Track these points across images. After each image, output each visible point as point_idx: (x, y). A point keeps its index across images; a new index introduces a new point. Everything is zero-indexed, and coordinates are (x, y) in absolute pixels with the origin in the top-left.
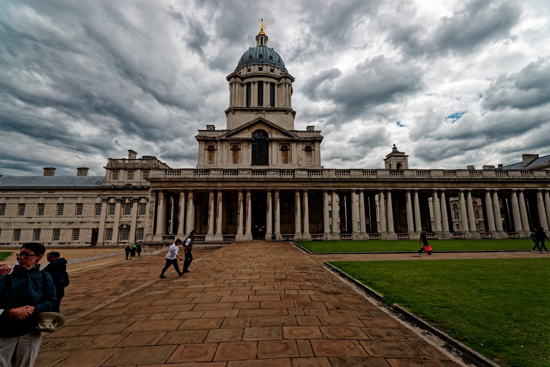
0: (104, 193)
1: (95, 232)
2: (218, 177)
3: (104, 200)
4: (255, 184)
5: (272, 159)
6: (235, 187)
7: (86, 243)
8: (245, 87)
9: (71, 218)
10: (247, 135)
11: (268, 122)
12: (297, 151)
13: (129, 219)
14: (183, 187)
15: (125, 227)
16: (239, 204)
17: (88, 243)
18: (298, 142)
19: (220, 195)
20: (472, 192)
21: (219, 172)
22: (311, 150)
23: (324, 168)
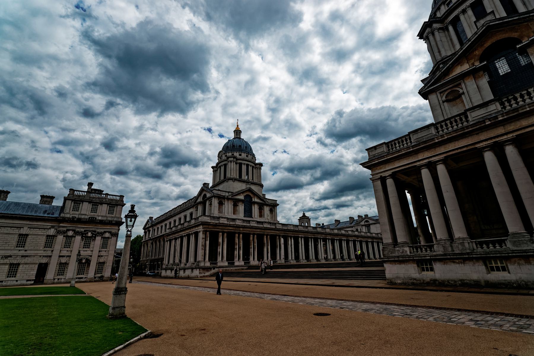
0: (61, 225)
1: (42, 269)
2: (240, 224)
3: (59, 232)
4: (259, 230)
5: (254, 214)
6: (250, 231)
7: (27, 280)
8: (238, 165)
9: (9, 252)
10: (241, 197)
11: (254, 191)
12: (267, 209)
13: (89, 253)
14: (221, 229)
15: (84, 261)
16: (251, 241)
17: (30, 280)
18: (267, 205)
19: (241, 235)
20: (323, 239)
21: (241, 221)
22: (273, 211)
23: (280, 223)
